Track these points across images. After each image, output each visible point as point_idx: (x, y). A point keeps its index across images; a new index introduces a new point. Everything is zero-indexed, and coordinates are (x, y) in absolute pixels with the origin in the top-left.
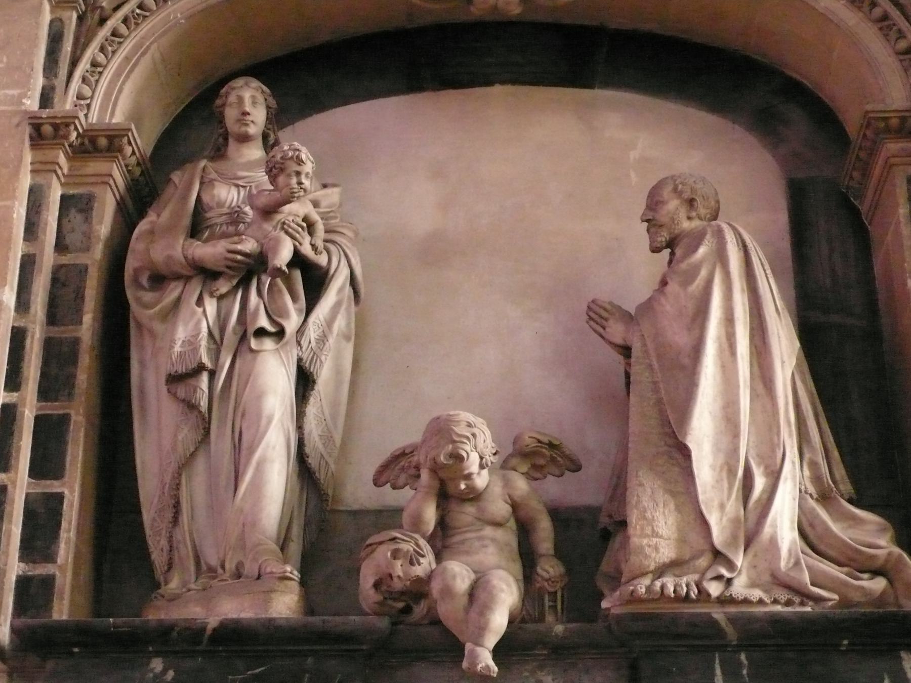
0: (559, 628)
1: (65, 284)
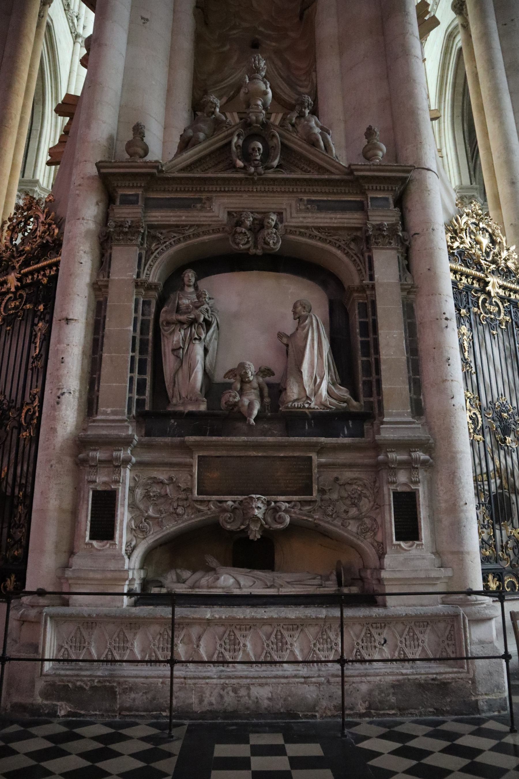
0: (269, 414)
1: (144, 324)
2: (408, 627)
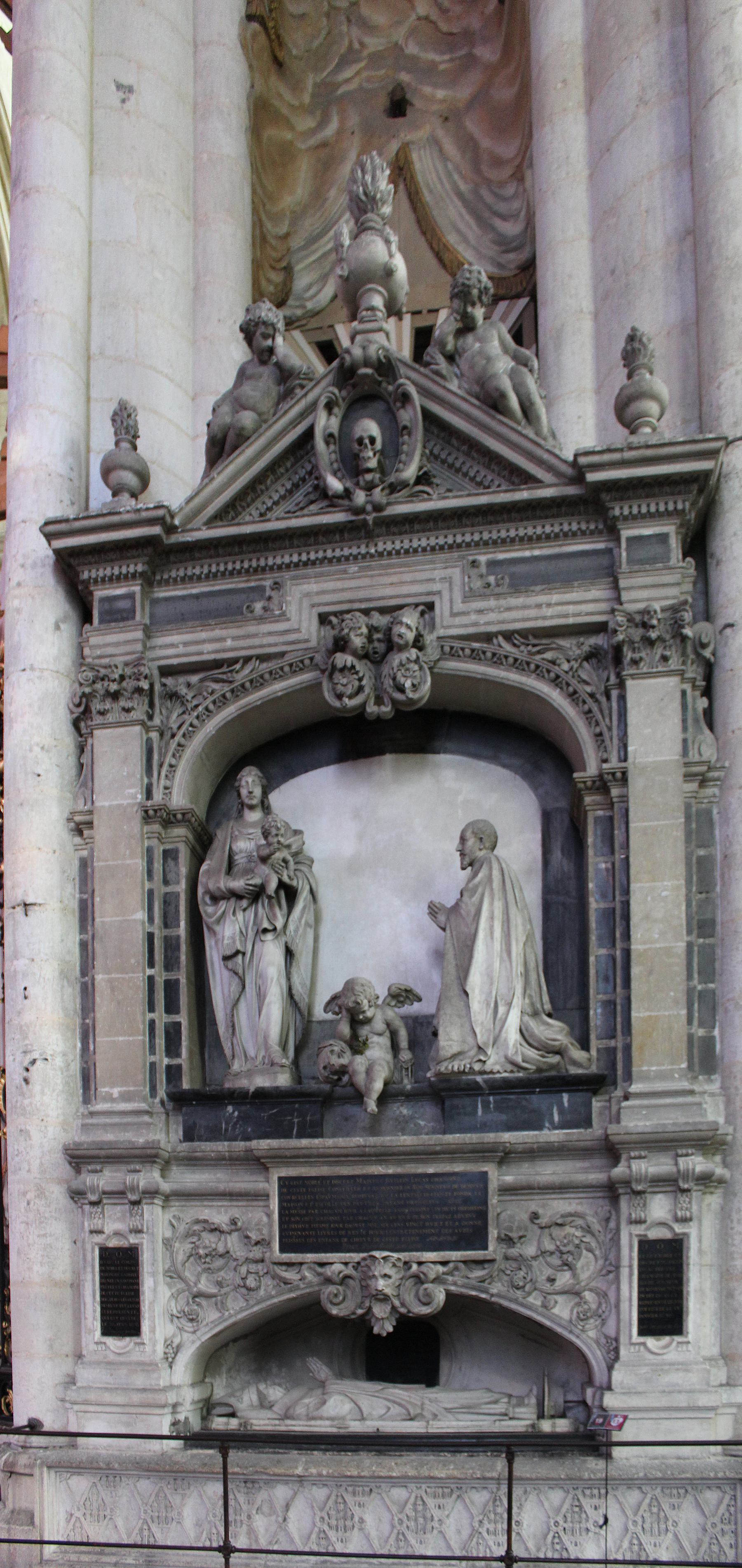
2: (649, 1496)
